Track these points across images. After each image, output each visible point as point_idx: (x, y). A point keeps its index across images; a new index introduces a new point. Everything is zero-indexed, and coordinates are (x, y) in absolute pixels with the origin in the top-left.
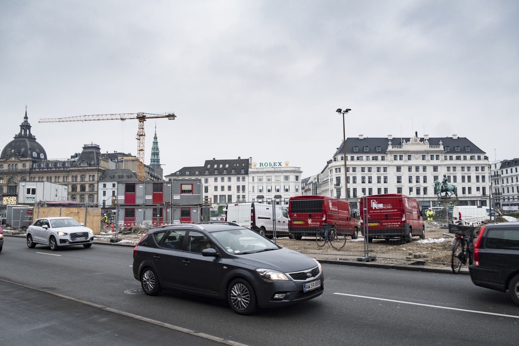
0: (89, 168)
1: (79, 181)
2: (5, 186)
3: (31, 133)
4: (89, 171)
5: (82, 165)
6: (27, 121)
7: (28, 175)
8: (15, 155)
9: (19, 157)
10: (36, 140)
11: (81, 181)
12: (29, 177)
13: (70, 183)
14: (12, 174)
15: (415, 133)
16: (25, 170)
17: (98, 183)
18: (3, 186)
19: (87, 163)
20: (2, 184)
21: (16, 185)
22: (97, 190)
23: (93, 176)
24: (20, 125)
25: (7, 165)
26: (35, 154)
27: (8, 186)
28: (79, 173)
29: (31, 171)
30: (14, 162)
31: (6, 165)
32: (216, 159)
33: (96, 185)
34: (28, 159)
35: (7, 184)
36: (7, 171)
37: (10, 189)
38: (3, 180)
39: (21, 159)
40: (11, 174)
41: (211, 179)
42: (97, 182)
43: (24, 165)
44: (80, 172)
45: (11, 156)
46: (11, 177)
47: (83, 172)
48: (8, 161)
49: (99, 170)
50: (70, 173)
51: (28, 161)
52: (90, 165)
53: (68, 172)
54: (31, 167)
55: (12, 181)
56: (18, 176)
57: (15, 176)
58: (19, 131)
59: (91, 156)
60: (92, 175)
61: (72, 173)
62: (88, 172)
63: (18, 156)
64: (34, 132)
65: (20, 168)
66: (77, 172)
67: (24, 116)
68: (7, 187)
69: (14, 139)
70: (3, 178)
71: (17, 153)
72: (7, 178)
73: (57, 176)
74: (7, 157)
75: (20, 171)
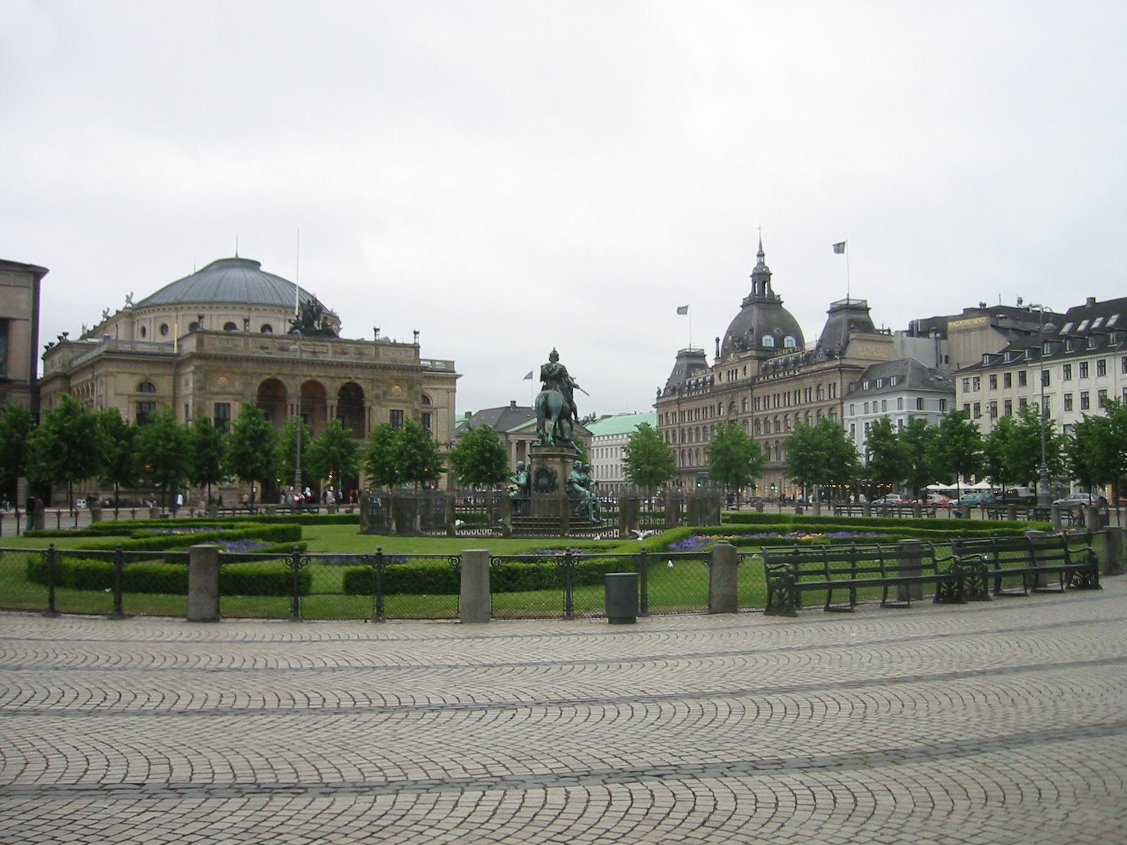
0: (826, 365)
3: (773, 289)
4: (827, 374)
5: (818, 359)
6: (761, 264)
7: (750, 391)
10: (783, 305)
15: (48, 268)
16: (747, 380)
17: (842, 403)
23: (835, 384)
24: (751, 273)
26: (768, 341)
29: (752, 384)
32: (1097, 301)
33: (839, 408)
34: (749, 354)
41: (1056, 372)
42: (839, 401)
44: (815, 376)
49: (840, 369)
52: (830, 356)
53: (795, 378)
54: (756, 374)
58: (750, 290)
60: (832, 383)
61: (805, 381)
62: (826, 377)
64: (777, 286)
69: (741, 309)
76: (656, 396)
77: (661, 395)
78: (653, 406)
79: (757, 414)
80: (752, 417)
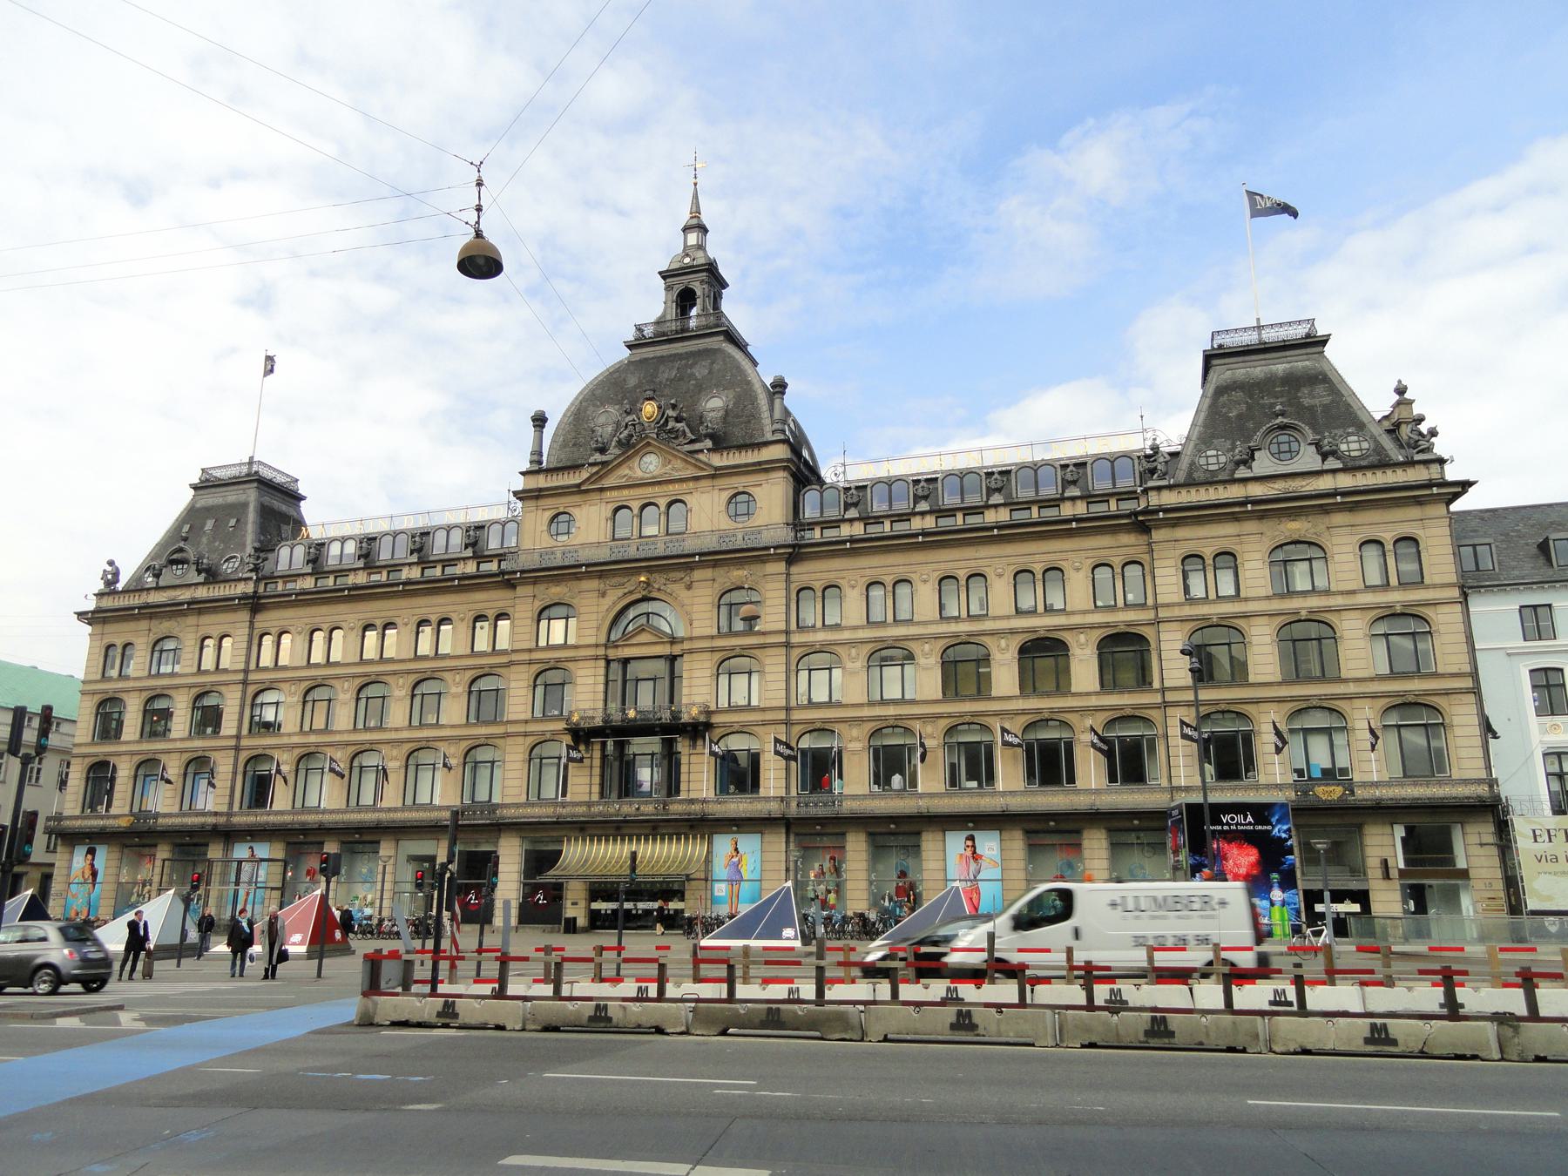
1: (1262, 592)
2: (586, 659)
7: (781, 567)
8: (664, 435)
9: (697, 446)
11: (1281, 596)
12: (788, 589)
13: (1176, 612)
14: (649, 570)
17: (1465, 595)
18: (574, 660)
19: (1318, 445)
20: (565, 646)
21: (677, 650)
22: (1465, 658)
25: (607, 510)
27: (608, 662)
28: (1250, 526)
30: (657, 489)
31: (593, 508)
33: (1446, 620)
35: (606, 646)
36: (603, 555)
37: (625, 682)
38: (567, 618)
39: (718, 460)
40: (638, 571)
43: (739, 502)
44: (1262, 516)
45: (630, 446)
46: (639, 596)
47: (1294, 513)
48: (607, 483)
50: (1157, 535)
51: (766, 470)
54: (791, 521)
55: (643, 620)
56: (689, 587)
57: (670, 587)
59: (1307, 402)
60: (1388, 537)
63: (692, 442)
65: (706, 527)
66: (1235, 518)
67: (684, 218)
68: (602, 671)
70: (574, 602)
71: (678, 419)
72: (607, 602)
73: (1038, 569)
74: (598, 457)
75: (711, 543)
76: (100, 586)
77: (120, 586)
78: (81, 615)
79: (821, 636)
80: (788, 645)
